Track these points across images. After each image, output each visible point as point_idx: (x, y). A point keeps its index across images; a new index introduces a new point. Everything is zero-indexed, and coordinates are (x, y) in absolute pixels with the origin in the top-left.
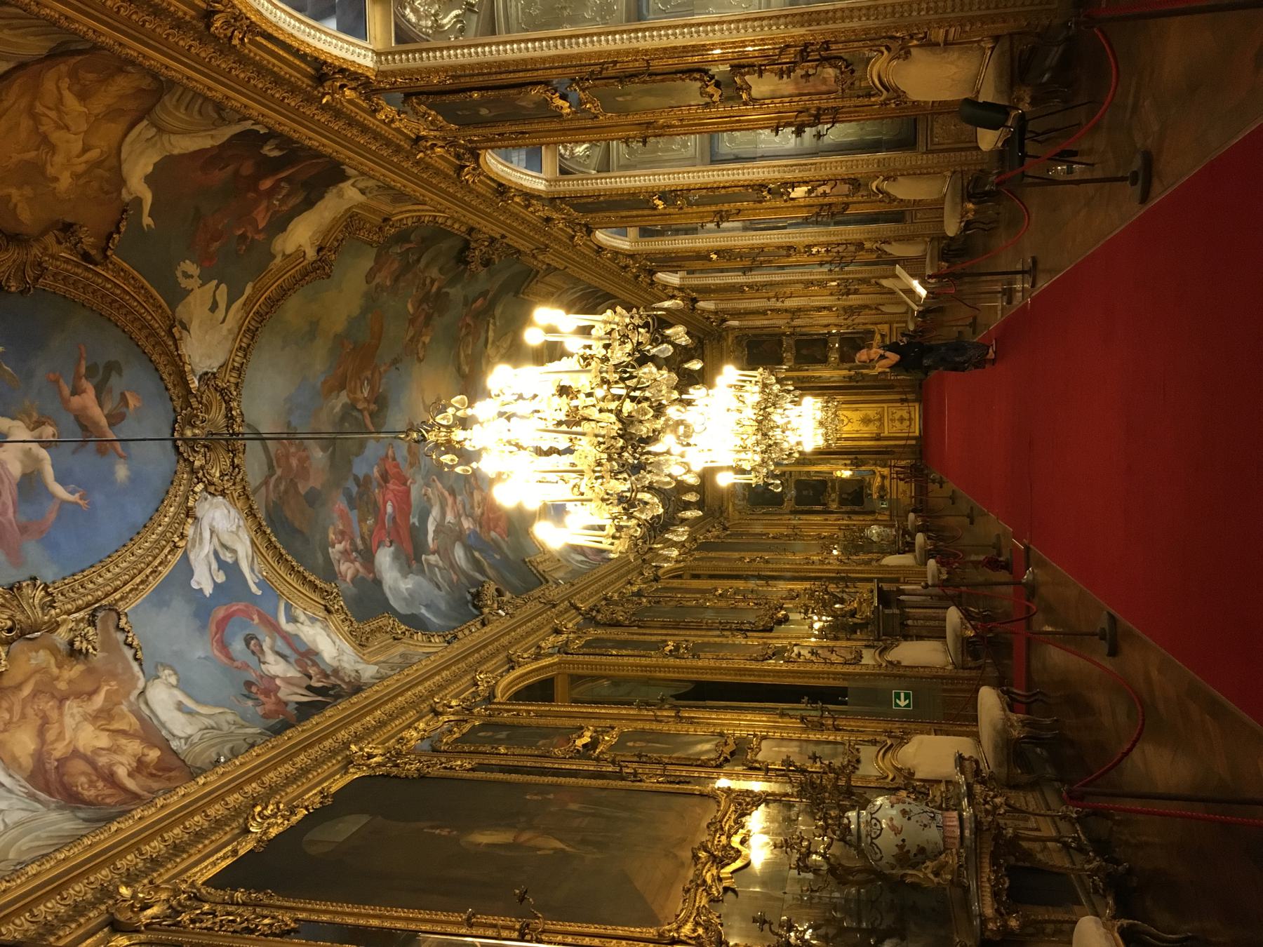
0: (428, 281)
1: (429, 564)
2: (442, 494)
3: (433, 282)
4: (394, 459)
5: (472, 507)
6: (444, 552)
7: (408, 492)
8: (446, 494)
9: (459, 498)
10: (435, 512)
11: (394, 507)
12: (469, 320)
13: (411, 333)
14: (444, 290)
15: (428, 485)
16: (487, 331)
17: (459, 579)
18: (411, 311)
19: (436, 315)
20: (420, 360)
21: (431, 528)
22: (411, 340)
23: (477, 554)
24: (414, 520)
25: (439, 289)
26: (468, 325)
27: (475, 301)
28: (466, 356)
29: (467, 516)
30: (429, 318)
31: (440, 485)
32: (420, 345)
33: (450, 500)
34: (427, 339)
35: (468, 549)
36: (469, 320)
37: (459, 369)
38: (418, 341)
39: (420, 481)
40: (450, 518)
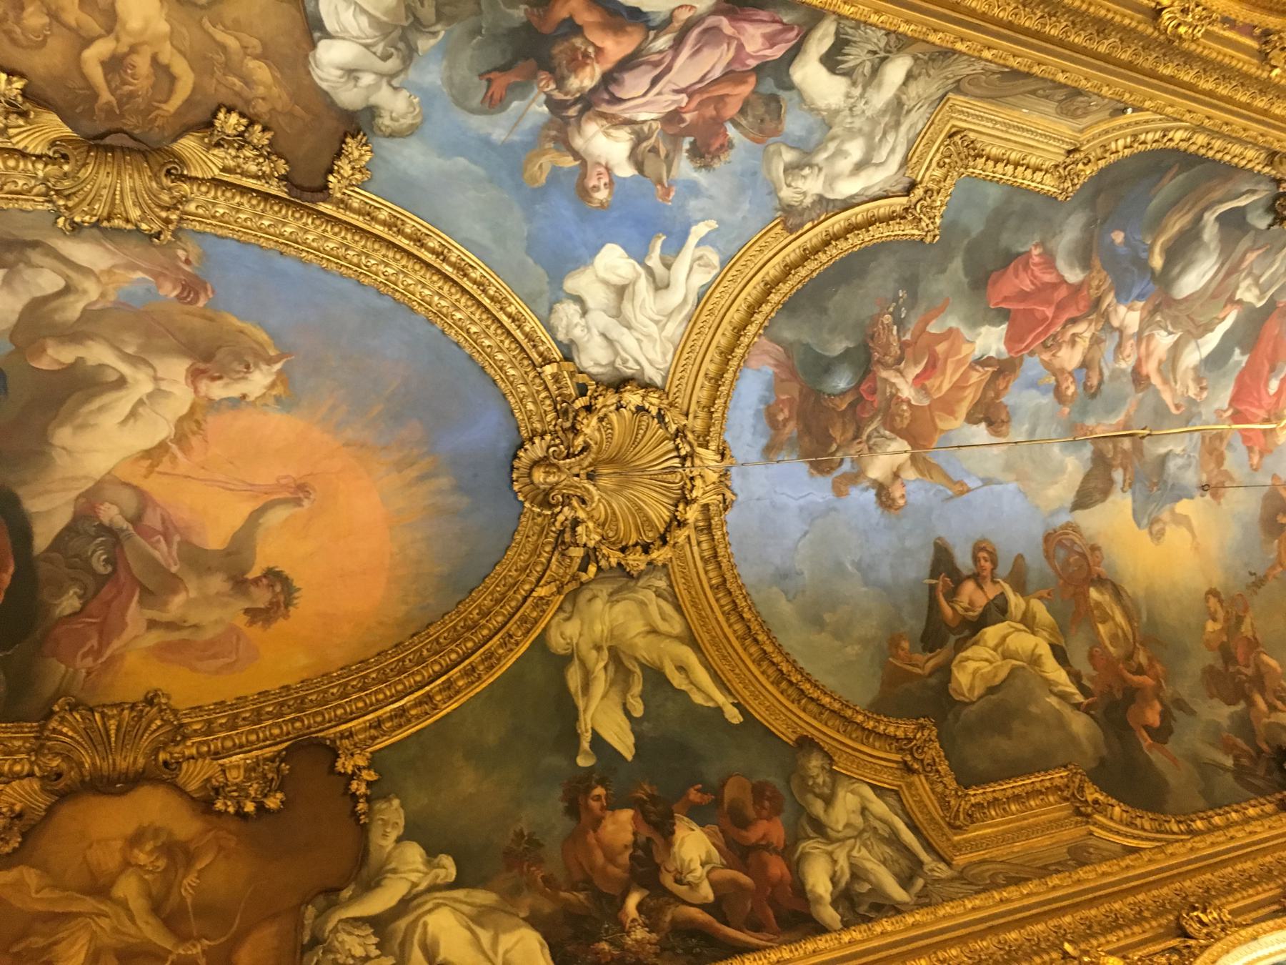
0: (1279, 704)
1: (1263, 293)
2: (1166, 381)
3: (1273, 708)
4: (1250, 449)
5: (1096, 341)
6: (1220, 293)
7: (1235, 400)
8: (1156, 380)
9: (1126, 365)
10: (1192, 356)
11: (1267, 385)
12: (1147, 680)
13: (1246, 629)
14: (1242, 705)
15: (1192, 402)
16: (1076, 677)
17: (1251, 249)
18: (1265, 658)
19: (1219, 665)
20: (1213, 593)
21: (1212, 341)
22: (1240, 620)
23: (1157, 262)
24: (1239, 358)
25: (1251, 703)
26: (1140, 671)
27: (1165, 715)
28: (1106, 618)
29: (1121, 331)
30: (1227, 655)
31: (1167, 397)
32: (1221, 614)
33: (1150, 368)
34: (1211, 626)
35: (1165, 280)
36: (1147, 680)
37: (1117, 592)
38: (1227, 620)
39: (1207, 412)
40: (1163, 340)
